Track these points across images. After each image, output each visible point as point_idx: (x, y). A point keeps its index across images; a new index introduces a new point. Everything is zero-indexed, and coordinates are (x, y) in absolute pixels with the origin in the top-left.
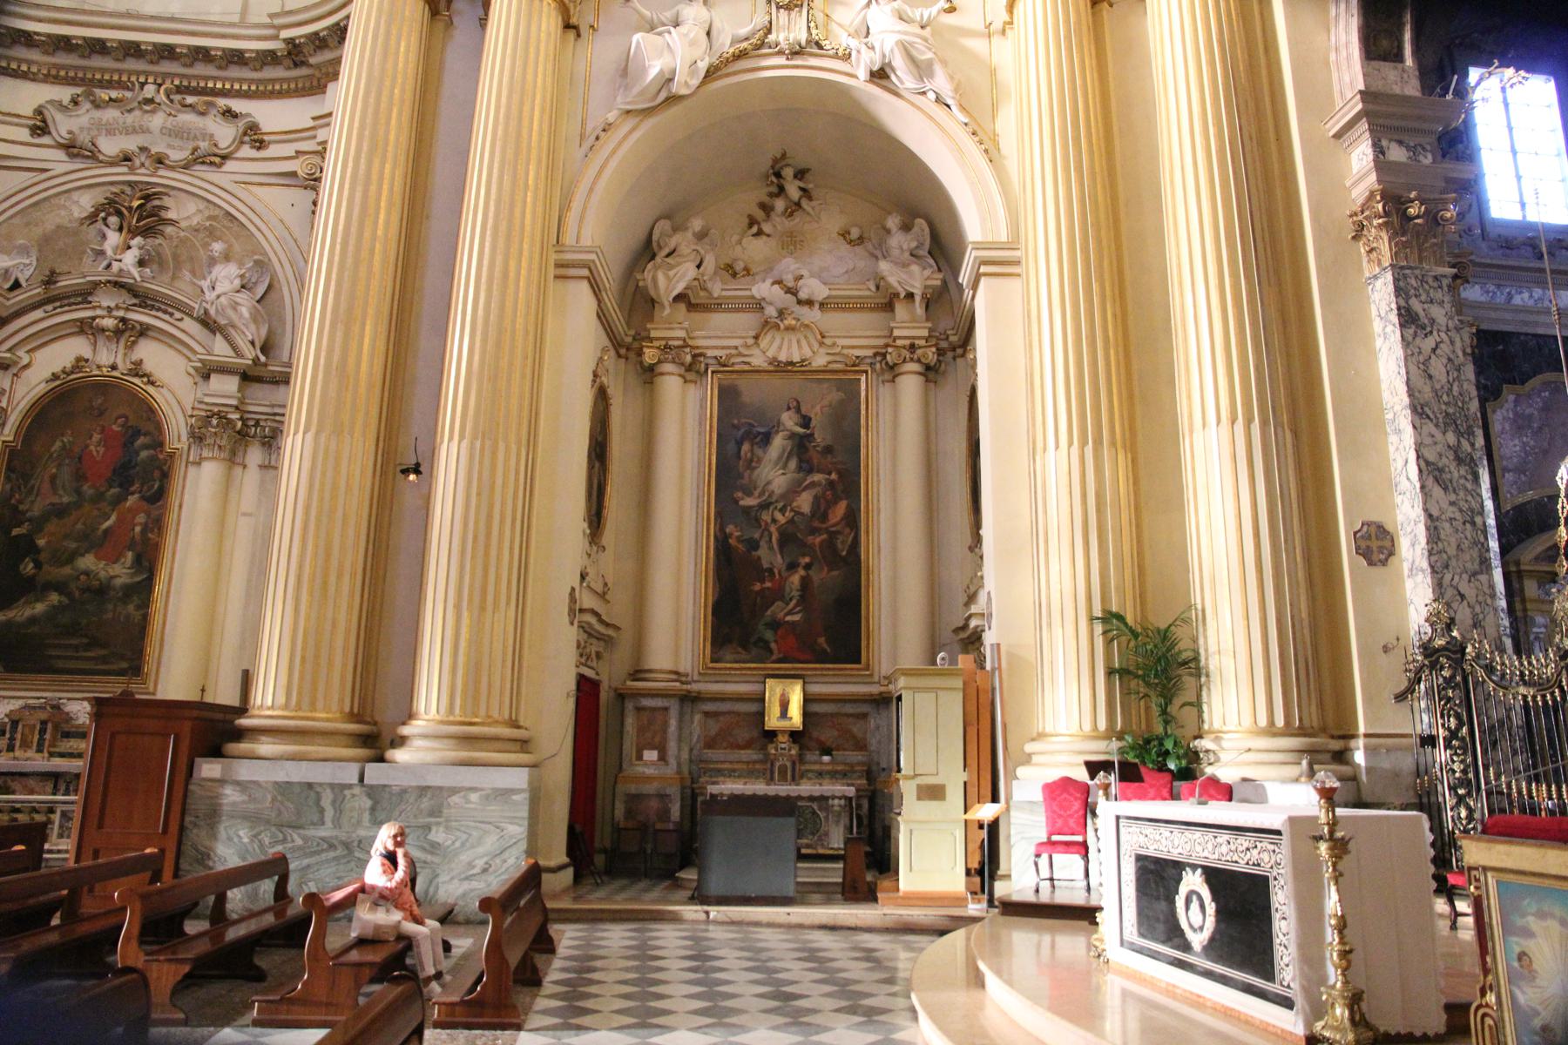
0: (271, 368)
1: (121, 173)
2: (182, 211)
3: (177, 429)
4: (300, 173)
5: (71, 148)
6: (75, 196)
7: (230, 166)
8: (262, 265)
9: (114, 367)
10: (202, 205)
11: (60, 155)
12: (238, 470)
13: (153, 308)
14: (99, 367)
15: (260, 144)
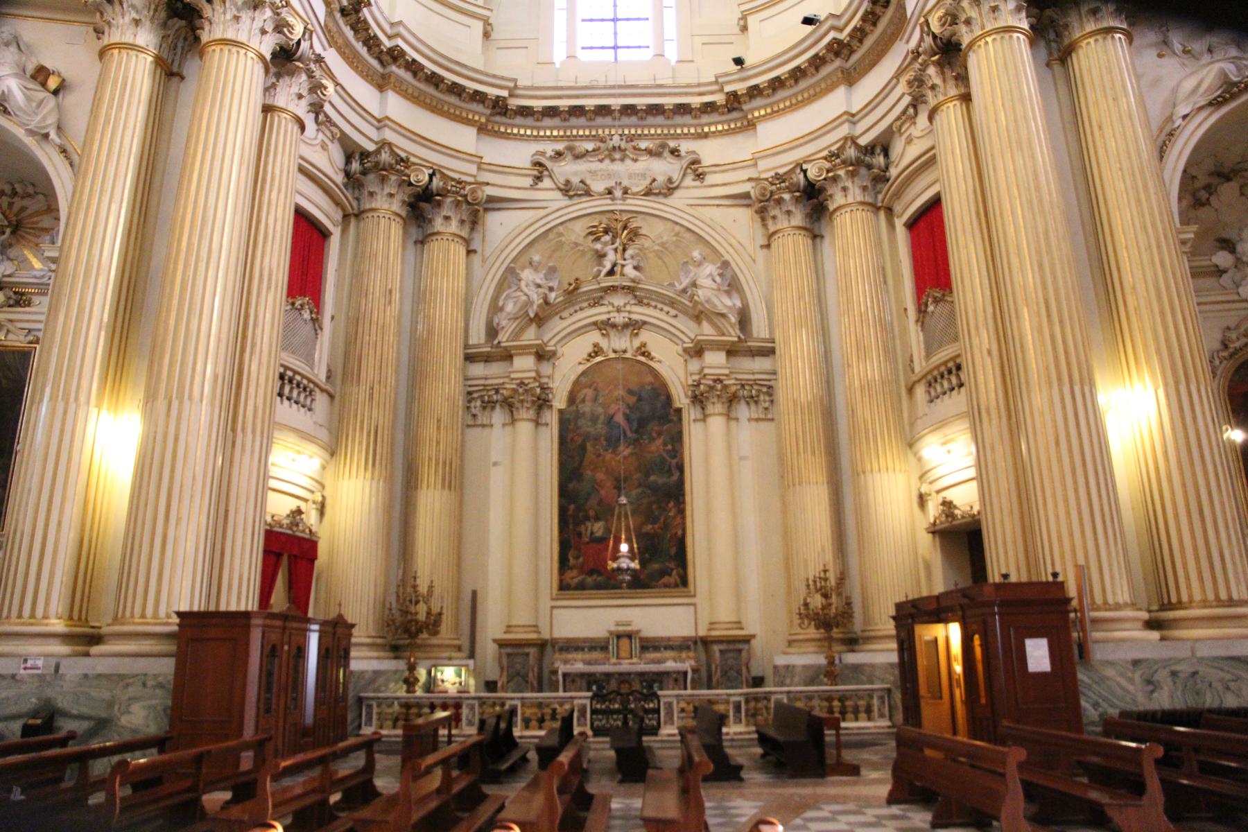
0: (749, 344)
1: (604, 204)
2: (652, 231)
3: (681, 399)
4: (752, 194)
5: (567, 190)
6: (569, 225)
7: (678, 194)
8: (726, 264)
9: (625, 351)
10: (669, 224)
11: (558, 195)
12: (733, 424)
13: (648, 305)
14: (615, 351)
15: (700, 176)
